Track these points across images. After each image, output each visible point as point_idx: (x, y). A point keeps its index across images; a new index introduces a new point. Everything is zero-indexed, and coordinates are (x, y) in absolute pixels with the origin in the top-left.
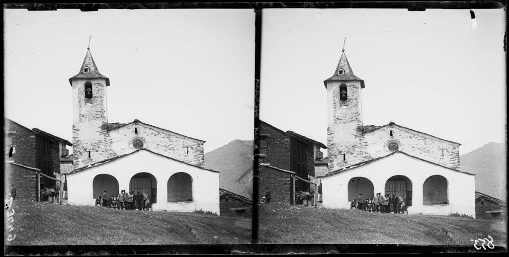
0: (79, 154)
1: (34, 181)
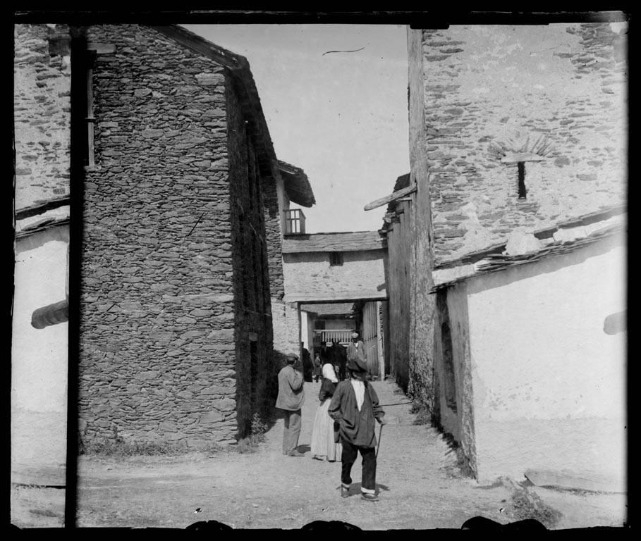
0: (462, 179)
1: (223, 325)
